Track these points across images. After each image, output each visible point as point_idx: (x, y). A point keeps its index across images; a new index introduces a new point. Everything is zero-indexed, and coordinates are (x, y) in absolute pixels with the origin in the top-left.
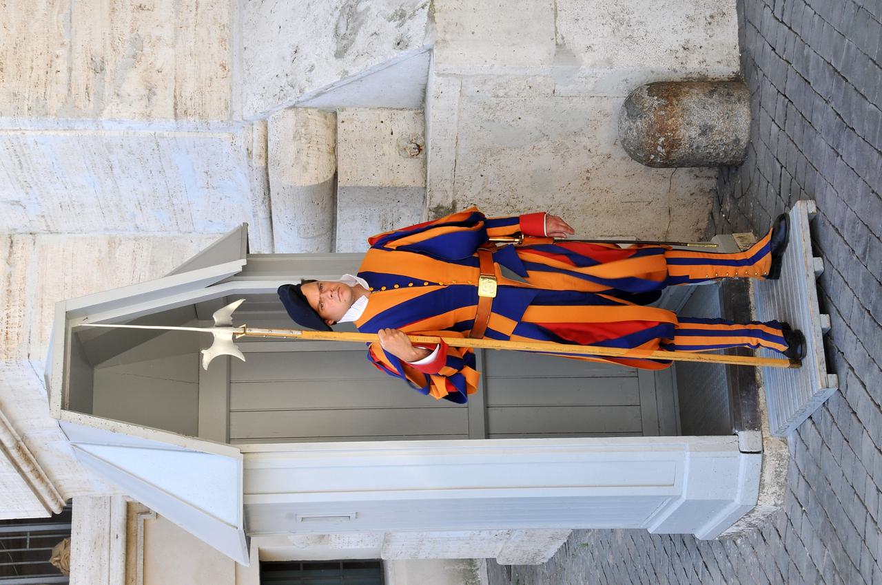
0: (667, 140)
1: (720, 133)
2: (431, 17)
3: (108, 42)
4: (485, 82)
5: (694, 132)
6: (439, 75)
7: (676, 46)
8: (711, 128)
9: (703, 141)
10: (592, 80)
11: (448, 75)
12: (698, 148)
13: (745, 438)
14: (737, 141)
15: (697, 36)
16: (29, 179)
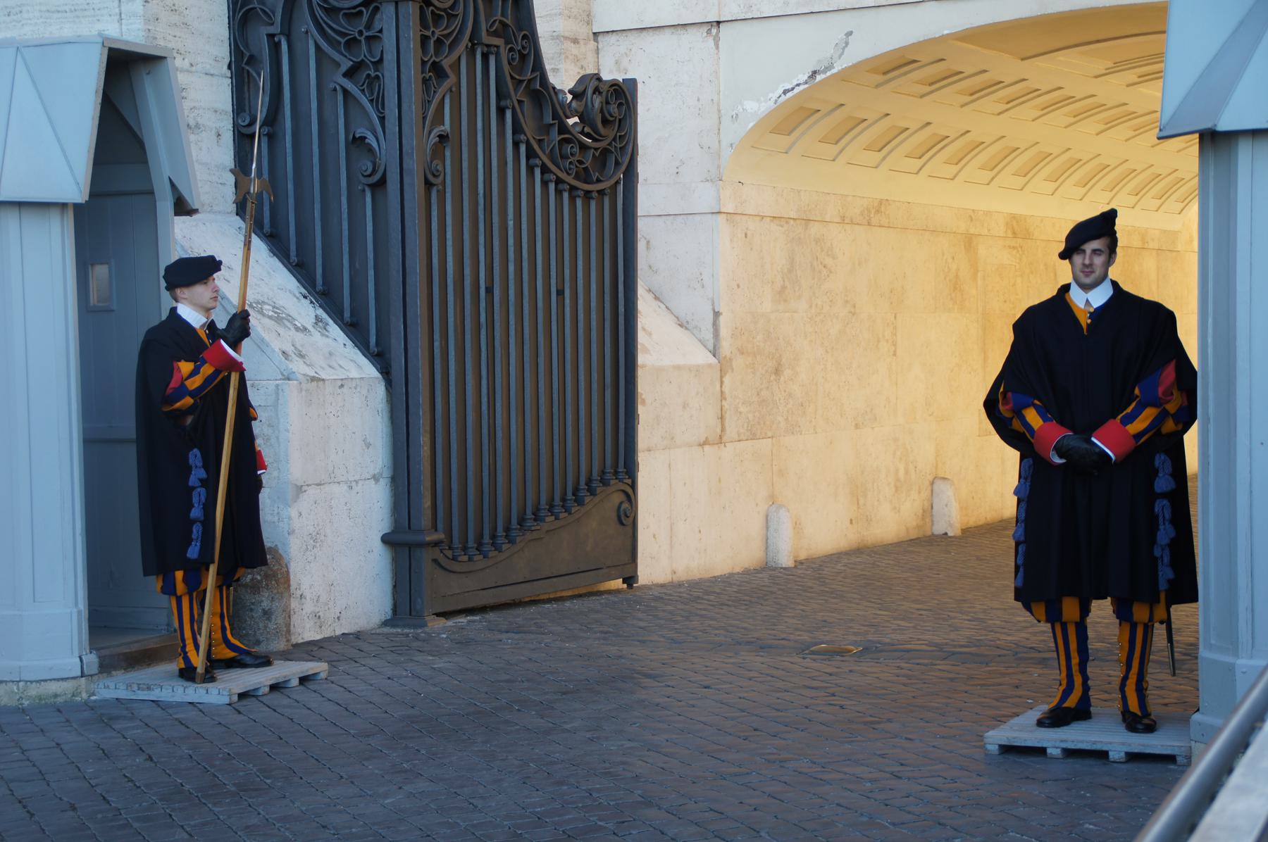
0: (260, 582)
1: (266, 627)
2: (313, 379)
3: (196, 104)
4: (270, 425)
5: (266, 604)
6: (277, 386)
7: (303, 587)
8: (269, 619)
9: (258, 613)
10: (276, 519)
11: (277, 394)
12: (251, 610)
13: (92, 659)
14: (258, 643)
15: (309, 607)
16: (25, 15)
